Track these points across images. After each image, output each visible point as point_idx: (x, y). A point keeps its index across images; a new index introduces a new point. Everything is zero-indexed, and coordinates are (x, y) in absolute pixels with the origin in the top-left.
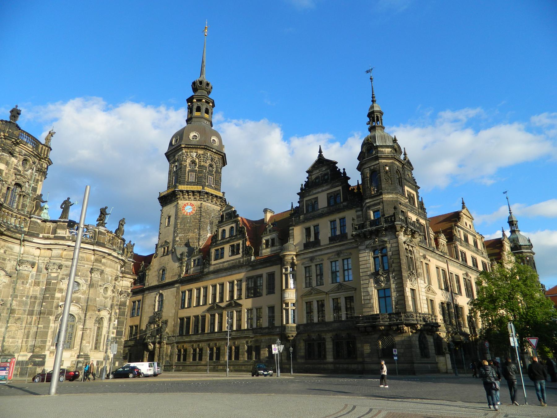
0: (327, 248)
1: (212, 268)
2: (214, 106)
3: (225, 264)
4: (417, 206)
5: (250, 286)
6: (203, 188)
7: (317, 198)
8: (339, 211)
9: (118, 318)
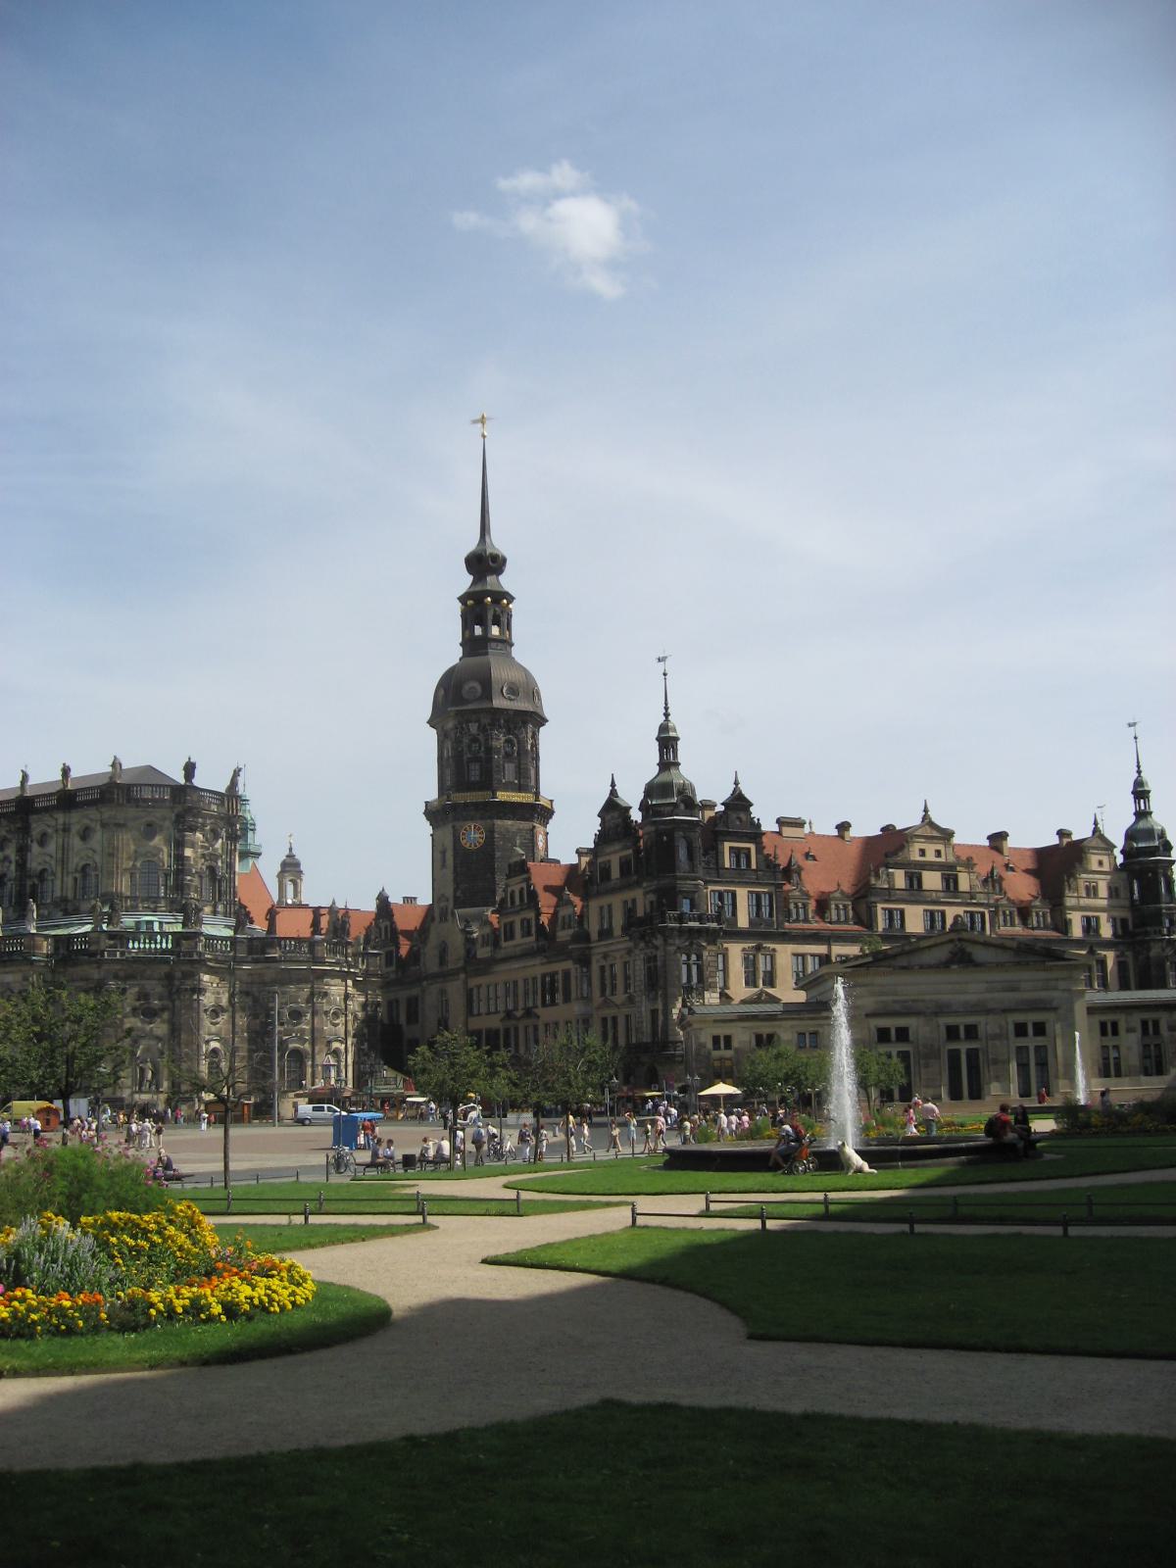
0: (618, 943)
2: (511, 599)
3: (518, 949)
4: (754, 867)
7: (609, 861)
8: (628, 887)
9: (366, 1041)
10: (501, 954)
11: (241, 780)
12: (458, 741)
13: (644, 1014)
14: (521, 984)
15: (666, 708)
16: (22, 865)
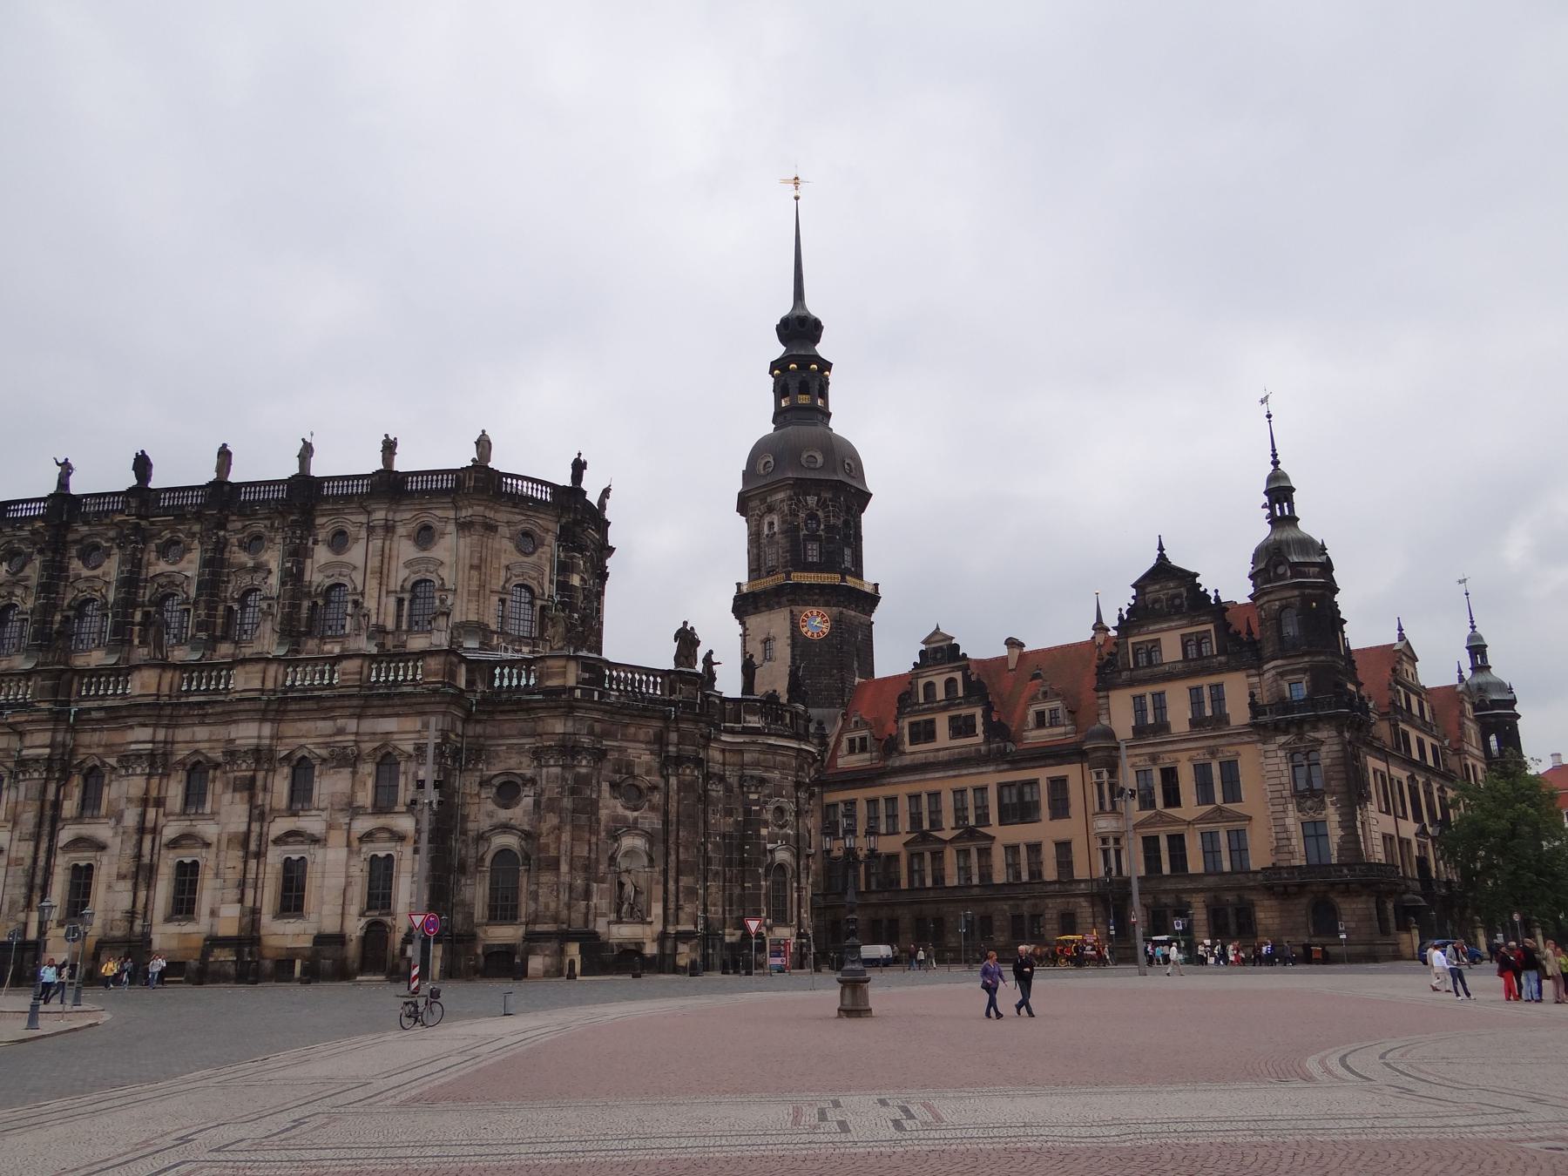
1: (907, 760)
5: (1006, 801)
6: (843, 579)
10: (896, 762)
11: (608, 502)
12: (794, 514)
13: (1292, 828)
14: (947, 802)
15: (1274, 455)
16: (293, 577)
